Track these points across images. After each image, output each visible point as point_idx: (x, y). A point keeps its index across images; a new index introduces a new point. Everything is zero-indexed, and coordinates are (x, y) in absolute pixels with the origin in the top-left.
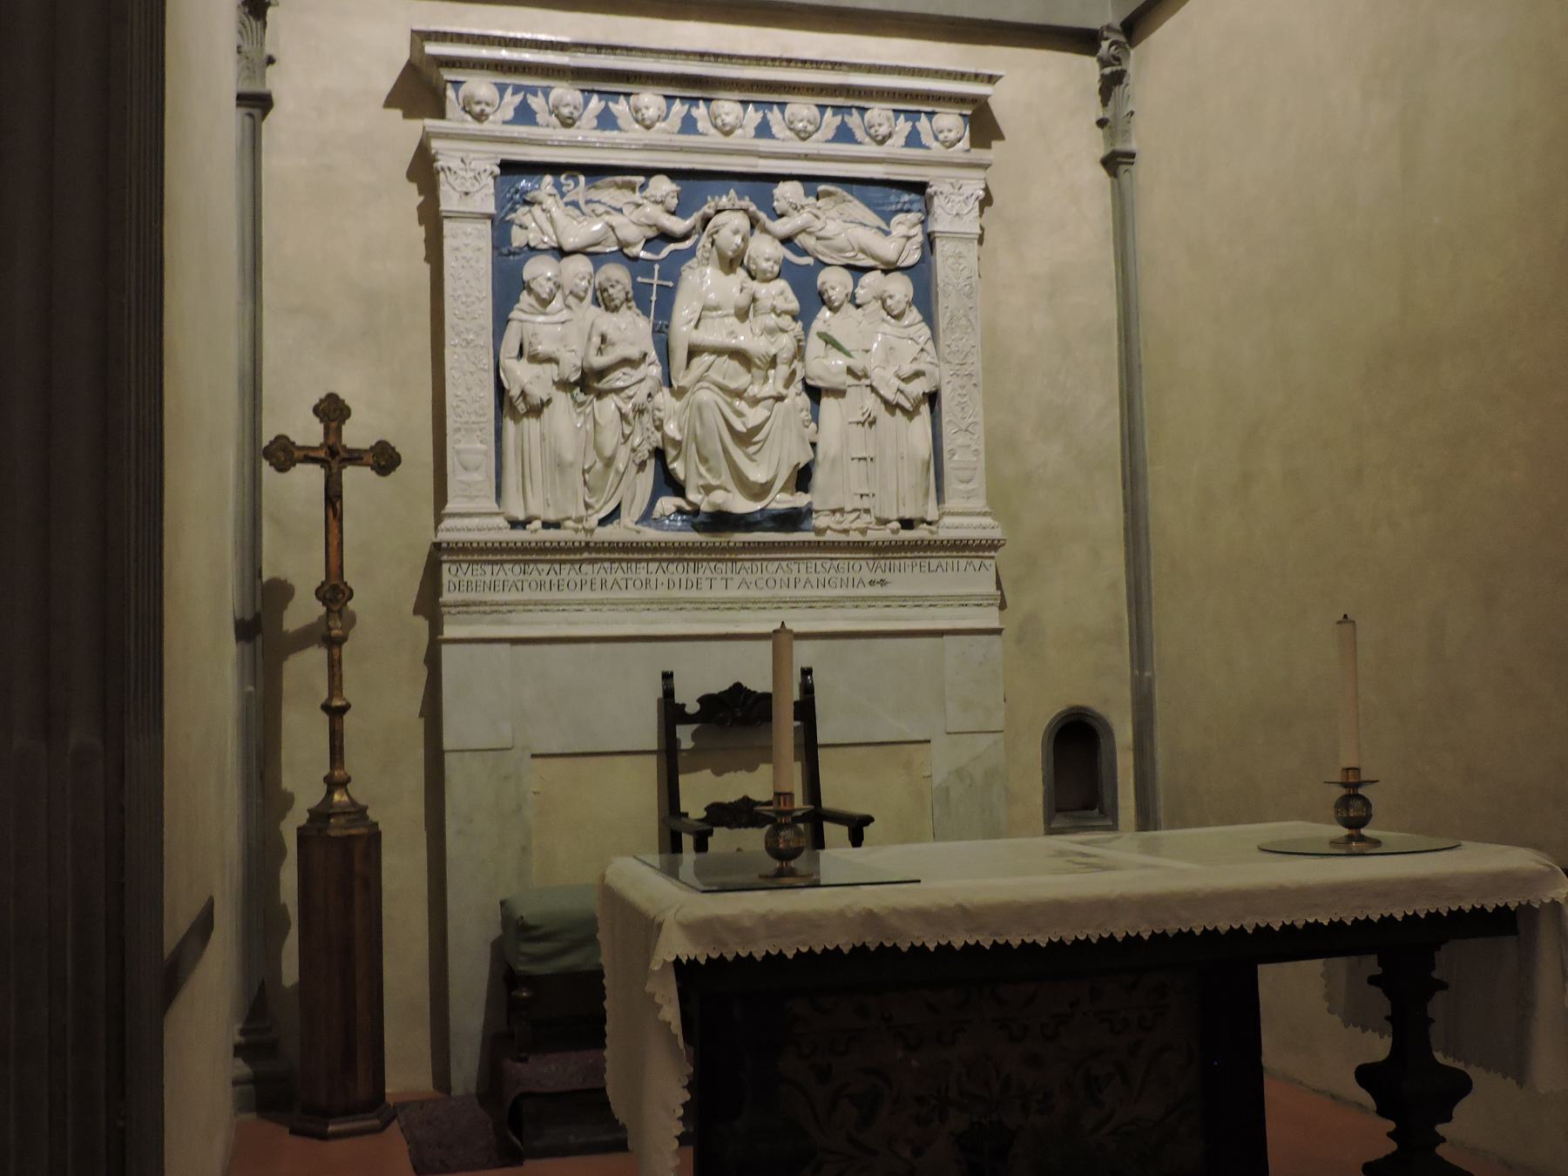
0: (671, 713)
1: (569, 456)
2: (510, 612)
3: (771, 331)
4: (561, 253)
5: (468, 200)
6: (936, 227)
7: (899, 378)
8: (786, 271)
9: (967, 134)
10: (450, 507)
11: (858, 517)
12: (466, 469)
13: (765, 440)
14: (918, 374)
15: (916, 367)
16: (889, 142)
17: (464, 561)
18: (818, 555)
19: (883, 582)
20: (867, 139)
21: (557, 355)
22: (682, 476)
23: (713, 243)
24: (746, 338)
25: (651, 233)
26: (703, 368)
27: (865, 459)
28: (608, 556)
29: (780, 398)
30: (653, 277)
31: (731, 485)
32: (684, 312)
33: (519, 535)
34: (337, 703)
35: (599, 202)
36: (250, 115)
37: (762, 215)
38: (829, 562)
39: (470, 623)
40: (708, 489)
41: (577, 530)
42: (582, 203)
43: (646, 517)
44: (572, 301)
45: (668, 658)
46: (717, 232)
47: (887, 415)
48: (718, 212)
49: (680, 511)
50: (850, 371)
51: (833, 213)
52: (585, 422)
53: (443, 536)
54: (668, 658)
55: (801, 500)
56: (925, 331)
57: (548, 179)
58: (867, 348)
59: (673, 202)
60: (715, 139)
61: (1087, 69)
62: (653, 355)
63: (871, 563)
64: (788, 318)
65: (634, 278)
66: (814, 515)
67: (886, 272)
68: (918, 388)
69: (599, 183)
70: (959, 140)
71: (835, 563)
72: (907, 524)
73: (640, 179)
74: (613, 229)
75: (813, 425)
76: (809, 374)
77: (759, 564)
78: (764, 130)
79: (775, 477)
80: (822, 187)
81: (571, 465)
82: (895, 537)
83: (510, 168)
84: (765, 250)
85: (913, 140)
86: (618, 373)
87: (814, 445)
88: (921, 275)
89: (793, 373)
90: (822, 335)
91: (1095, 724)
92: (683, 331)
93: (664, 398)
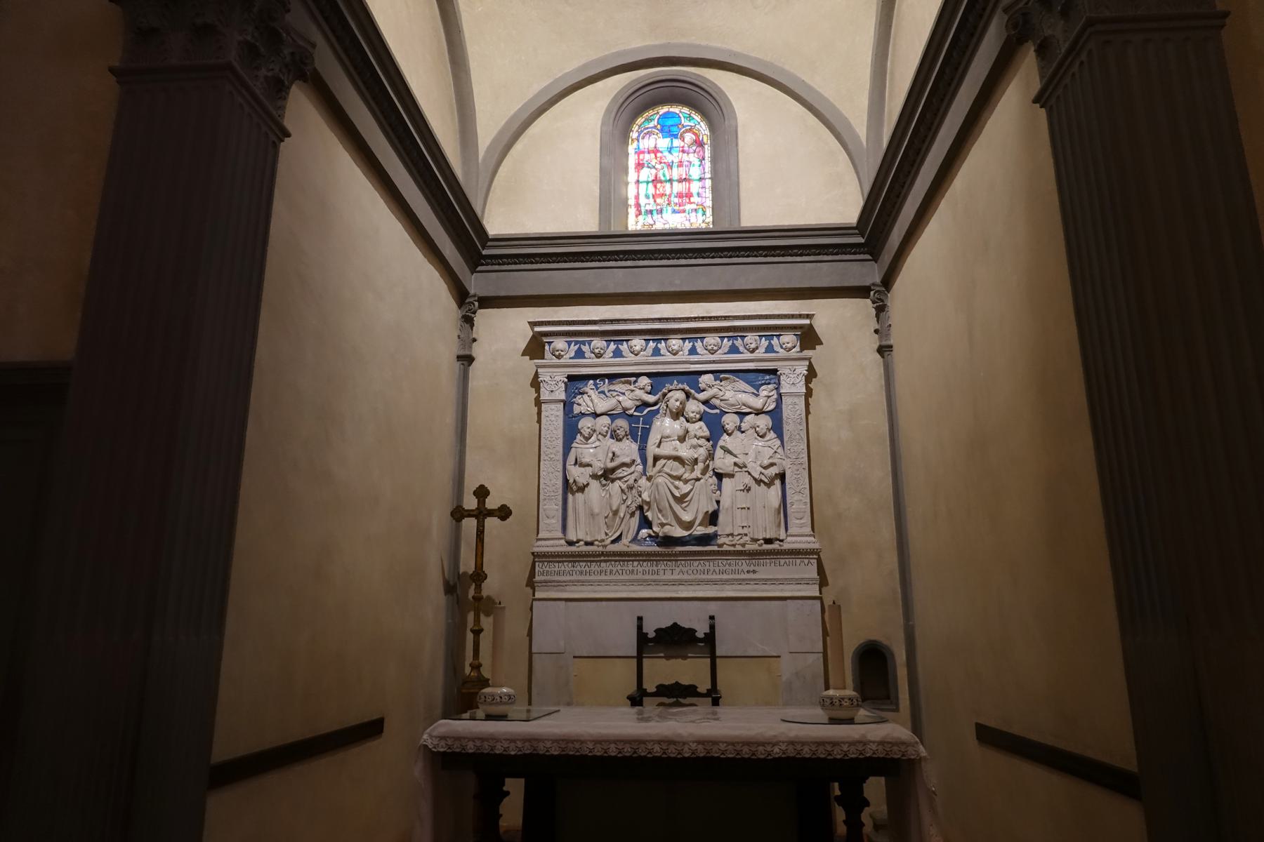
1: (596, 510)
2: (566, 585)
3: (695, 447)
4: (596, 415)
5: (553, 394)
7: (762, 467)
8: (703, 417)
9: (798, 344)
10: (540, 536)
11: (741, 538)
12: (548, 517)
13: (691, 500)
14: (772, 465)
15: (771, 461)
16: (757, 351)
17: (545, 561)
18: (719, 558)
19: (754, 572)
20: (746, 351)
21: (592, 462)
22: (650, 519)
23: (667, 406)
24: (685, 451)
25: (638, 403)
26: (660, 467)
27: (744, 508)
28: (613, 558)
29: (698, 479)
30: (639, 424)
31: (674, 523)
32: (653, 438)
34: (476, 628)
35: (614, 391)
36: (463, 364)
37: (693, 391)
38: (725, 561)
39: (547, 591)
41: (598, 546)
42: (606, 392)
43: (635, 540)
44: (600, 437)
46: (668, 401)
48: (670, 391)
49: (650, 536)
50: (735, 464)
51: (729, 388)
52: (606, 494)
53: (536, 550)
54: (640, 609)
55: (711, 530)
56: (778, 442)
57: (591, 382)
58: (747, 452)
61: (865, 306)
62: (639, 461)
63: (748, 561)
65: (630, 425)
66: (718, 537)
67: (757, 414)
68: (773, 471)
69: (614, 382)
70: (794, 347)
71: (729, 562)
72: (769, 541)
73: (634, 379)
74: (620, 402)
75: (718, 492)
76: (716, 467)
77: (689, 562)
78: (693, 351)
79: (695, 518)
81: (598, 515)
82: (760, 548)
83: (571, 378)
85: (770, 349)
86: (620, 471)
87: (718, 502)
88: (776, 415)
89: (708, 465)
90: (722, 447)
92: (652, 449)
93: (643, 481)
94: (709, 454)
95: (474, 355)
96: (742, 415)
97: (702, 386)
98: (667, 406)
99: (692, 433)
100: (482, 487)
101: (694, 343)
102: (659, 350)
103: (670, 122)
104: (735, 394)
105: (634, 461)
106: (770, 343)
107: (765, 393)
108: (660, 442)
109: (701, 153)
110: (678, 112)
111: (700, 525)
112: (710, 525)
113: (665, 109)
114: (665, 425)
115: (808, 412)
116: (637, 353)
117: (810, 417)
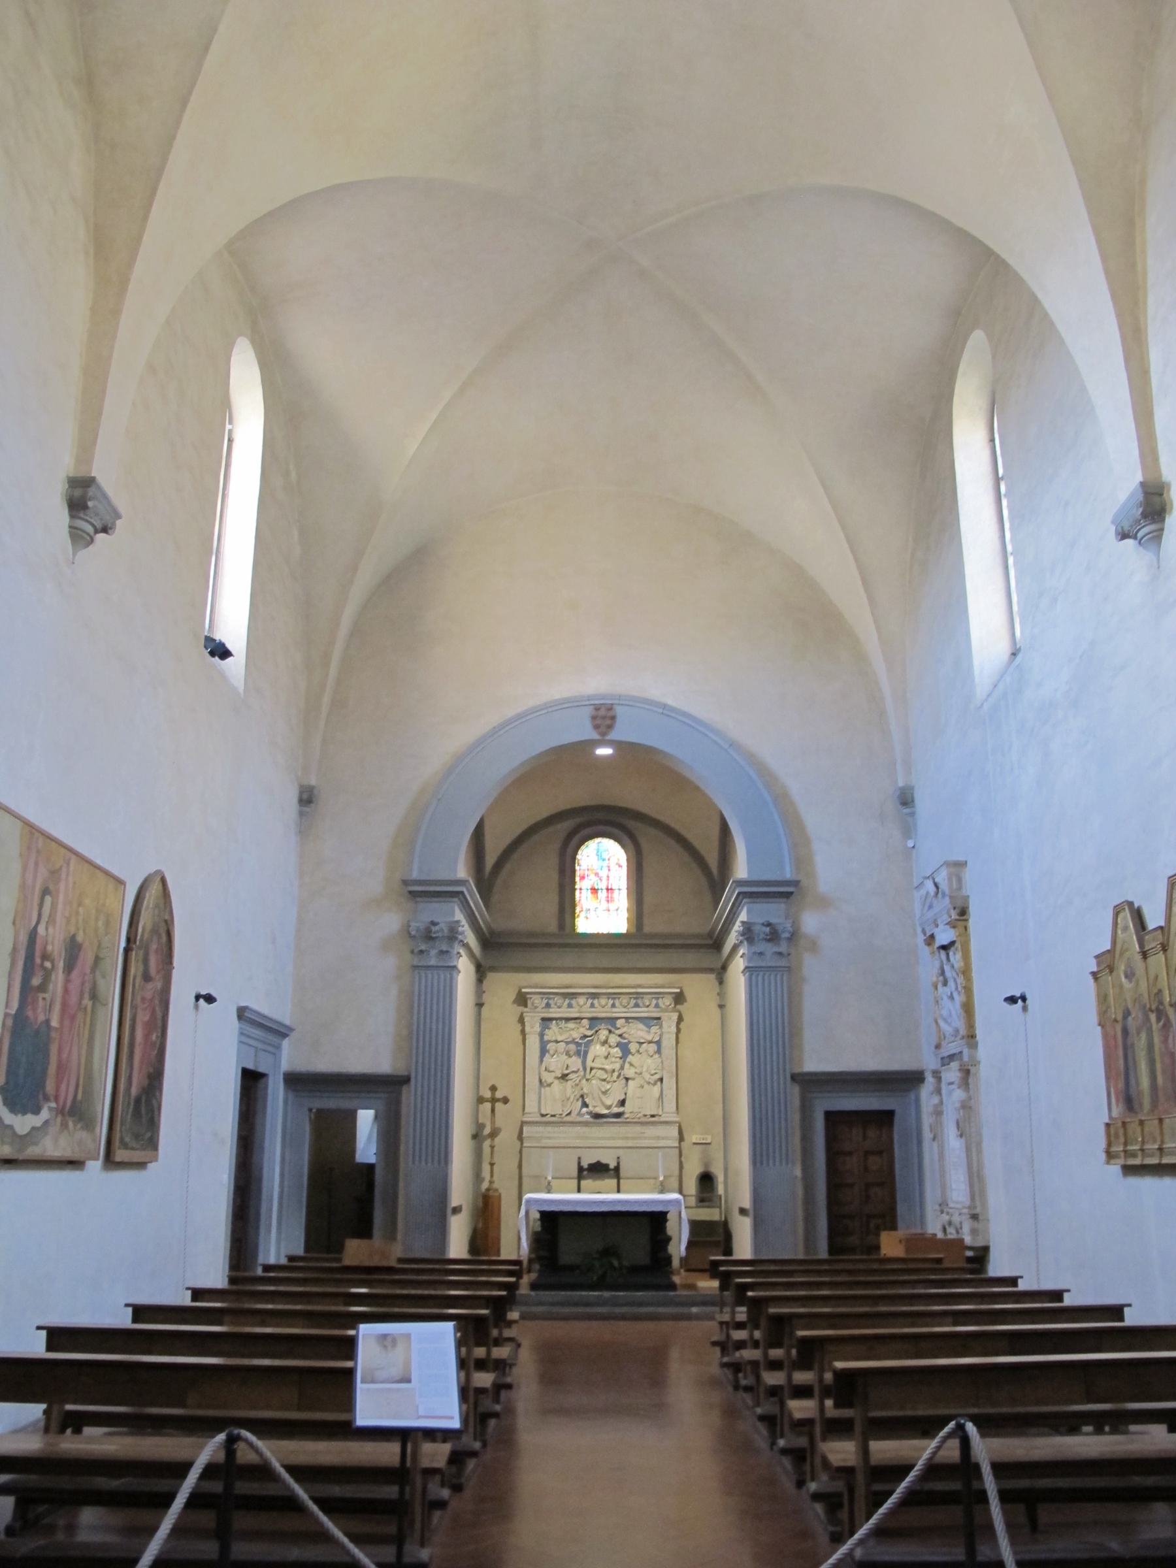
0: (581, 1169)
4: (557, 1042)
8: (618, 1045)
10: (526, 1111)
13: (610, 1094)
14: (656, 1073)
15: (655, 1071)
29: (615, 1082)
33: (544, 1119)
34: (493, 1162)
37: (613, 1029)
40: (595, 1107)
42: (563, 1028)
43: (579, 1114)
44: (560, 1055)
45: (579, 1152)
49: (587, 1113)
50: (636, 1073)
54: (579, 1152)
55: (621, 1110)
59: (588, 1027)
60: (600, 1009)
62: (581, 1069)
68: (657, 1076)
70: (670, 1005)
72: (653, 1116)
73: (578, 1021)
78: (613, 1006)
79: (613, 1104)
80: (630, 1021)
83: (543, 1019)
84: (613, 1039)
87: (626, 1094)
88: (658, 1043)
92: (589, 1064)
96: (641, 1043)
97: (618, 1026)
104: (637, 1032)
105: (579, 1070)
108: (594, 1059)
114: (597, 1050)
116: (582, 1008)
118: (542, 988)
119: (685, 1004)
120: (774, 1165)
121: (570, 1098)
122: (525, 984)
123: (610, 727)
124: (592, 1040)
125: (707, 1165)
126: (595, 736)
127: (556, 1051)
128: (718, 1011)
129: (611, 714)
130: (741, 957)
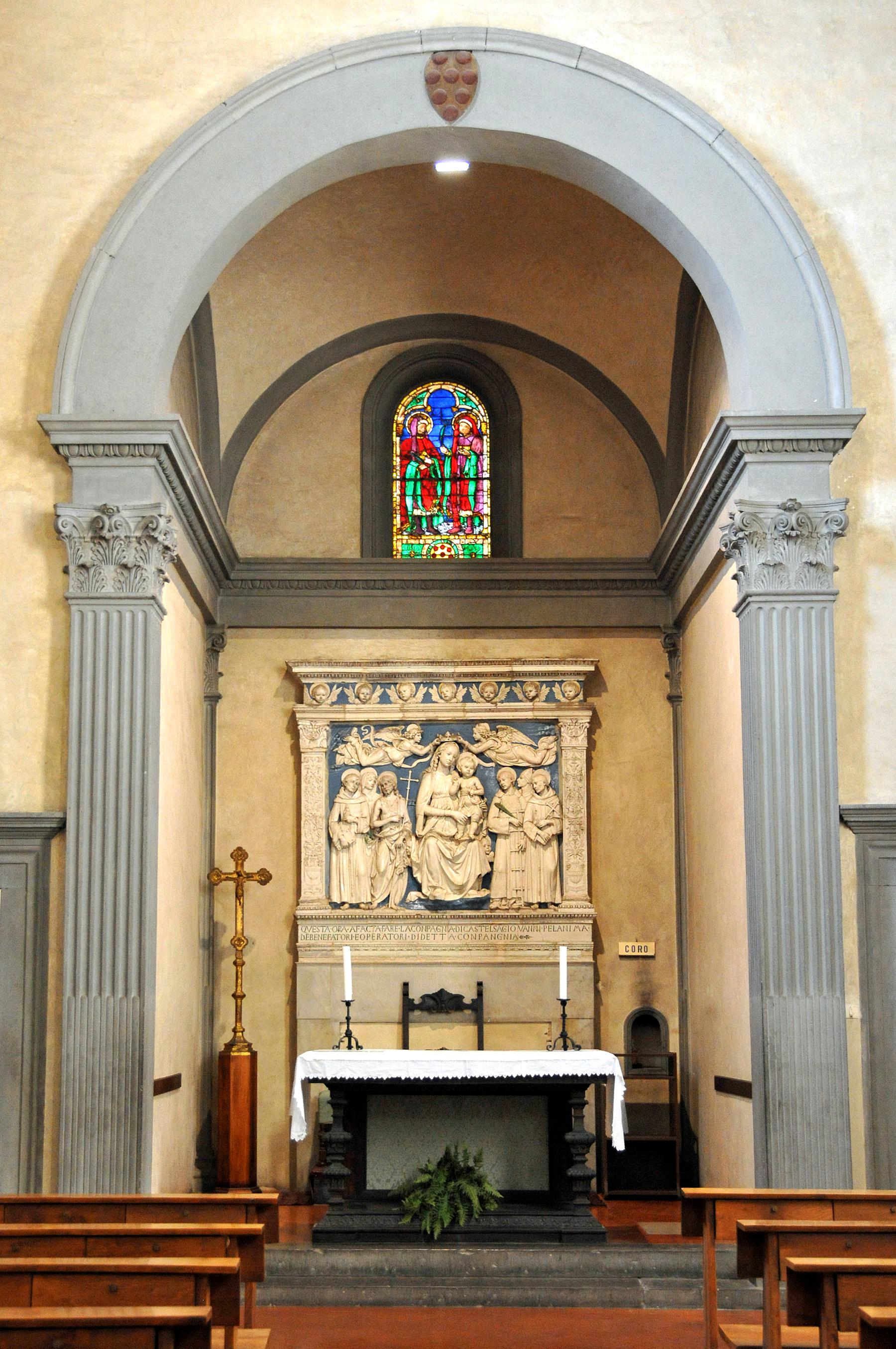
4: (360, 767)
6: (563, 744)
10: (301, 899)
14: (549, 825)
15: (548, 821)
16: (537, 699)
20: (525, 699)
22: (419, 880)
23: (439, 759)
25: (407, 755)
29: (471, 840)
31: (445, 886)
37: (466, 743)
43: (404, 903)
45: (406, 974)
47: (533, 848)
48: (442, 743)
49: (419, 899)
55: (483, 893)
59: (418, 738)
60: (442, 704)
62: (407, 819)
63: (521, 926)
64: (477, 798)
65: (398, 778)
67: (535, 769)
70: (577, 696)
71: (501, 926)
75: (492, 853)
78: (467, 698)
79: (468, 881)
84: (468, 762)
86: (388, 829)
87: (491, 864)
88: (554, 768)
89: (482, 824)
90: (497, 805)
91: (657, 1017)
92: (422, 807)
94: (483, 812)
95: (220, 691)
96: (519, 769)
97: (477, 736)
98: (439, 759)
99: (464, 789)
100: (240, 849)
101: (468, 689)
102: (431, 695)
103: (442, 404)
106: (551, 690)
107: (545, 745)
109: (479, 445)
110: (452, 391)
111: (471, 889)
112: (483, 888)
113: (434, 387)
115: (589, 767)
117: (592, 772)
118: (330, 663)
119: (604, 695)
120: (806, 990)
121: (385, 871)
122: (299, 659)
123: (466, 100)
124: (428, 764)
125: (646, 995)
126: (434, 120)
127: (360, 784)
128: (668, 707)
129: (467, 70)
130: (735, 577)
